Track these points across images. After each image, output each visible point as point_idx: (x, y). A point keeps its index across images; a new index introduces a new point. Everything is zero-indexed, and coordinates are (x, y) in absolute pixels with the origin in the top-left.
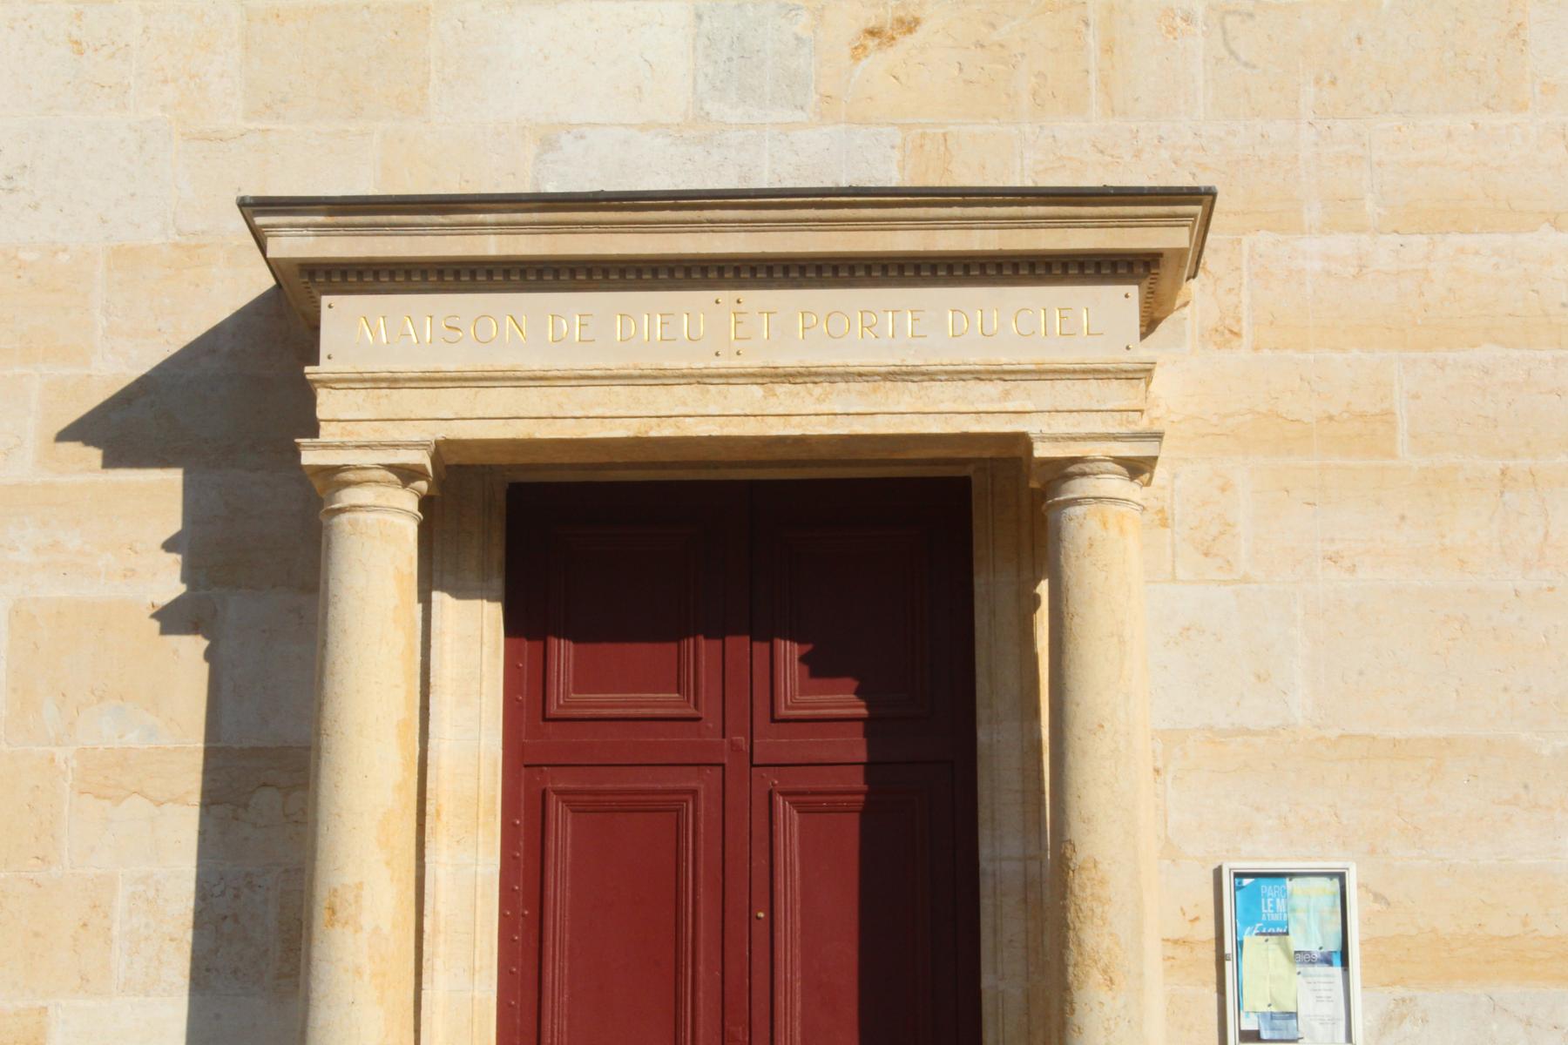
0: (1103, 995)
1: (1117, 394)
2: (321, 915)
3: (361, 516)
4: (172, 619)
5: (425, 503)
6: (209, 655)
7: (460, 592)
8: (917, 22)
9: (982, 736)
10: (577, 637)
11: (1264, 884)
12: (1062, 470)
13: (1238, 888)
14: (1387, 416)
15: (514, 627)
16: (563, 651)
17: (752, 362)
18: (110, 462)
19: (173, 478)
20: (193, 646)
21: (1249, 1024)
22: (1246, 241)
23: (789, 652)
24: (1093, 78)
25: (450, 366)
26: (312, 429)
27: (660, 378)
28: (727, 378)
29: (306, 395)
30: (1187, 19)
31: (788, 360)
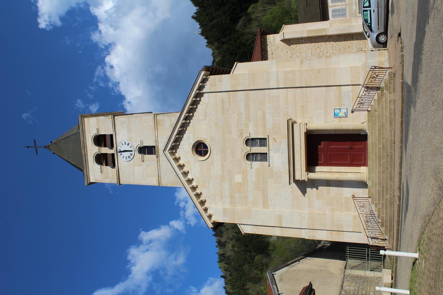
0: (343, 127)
1: (301, 126)
2: (338, 179)
3: (311, 176)
4: (317, 189)
5: (310, 172)
7: (315, 169)
9: (325, 134)
10: (318, 161)
11: (335, 114)
12: (307, 130)
13: (335, 116)
14: (302, 105)
15: (317, 166)
16: (319, 162)
17: (300, 151)
18: (306, 193)
19: (307, 189)
20: (319, 187)
21: (345, 115)
22: (289, 115)
23: (319, 147)
25: (300, 171)
26: (305, 180)
27: (301, 157)
28: (301, 152)
29: (302, 180)
30: (273, 119)
31: (300, 148)
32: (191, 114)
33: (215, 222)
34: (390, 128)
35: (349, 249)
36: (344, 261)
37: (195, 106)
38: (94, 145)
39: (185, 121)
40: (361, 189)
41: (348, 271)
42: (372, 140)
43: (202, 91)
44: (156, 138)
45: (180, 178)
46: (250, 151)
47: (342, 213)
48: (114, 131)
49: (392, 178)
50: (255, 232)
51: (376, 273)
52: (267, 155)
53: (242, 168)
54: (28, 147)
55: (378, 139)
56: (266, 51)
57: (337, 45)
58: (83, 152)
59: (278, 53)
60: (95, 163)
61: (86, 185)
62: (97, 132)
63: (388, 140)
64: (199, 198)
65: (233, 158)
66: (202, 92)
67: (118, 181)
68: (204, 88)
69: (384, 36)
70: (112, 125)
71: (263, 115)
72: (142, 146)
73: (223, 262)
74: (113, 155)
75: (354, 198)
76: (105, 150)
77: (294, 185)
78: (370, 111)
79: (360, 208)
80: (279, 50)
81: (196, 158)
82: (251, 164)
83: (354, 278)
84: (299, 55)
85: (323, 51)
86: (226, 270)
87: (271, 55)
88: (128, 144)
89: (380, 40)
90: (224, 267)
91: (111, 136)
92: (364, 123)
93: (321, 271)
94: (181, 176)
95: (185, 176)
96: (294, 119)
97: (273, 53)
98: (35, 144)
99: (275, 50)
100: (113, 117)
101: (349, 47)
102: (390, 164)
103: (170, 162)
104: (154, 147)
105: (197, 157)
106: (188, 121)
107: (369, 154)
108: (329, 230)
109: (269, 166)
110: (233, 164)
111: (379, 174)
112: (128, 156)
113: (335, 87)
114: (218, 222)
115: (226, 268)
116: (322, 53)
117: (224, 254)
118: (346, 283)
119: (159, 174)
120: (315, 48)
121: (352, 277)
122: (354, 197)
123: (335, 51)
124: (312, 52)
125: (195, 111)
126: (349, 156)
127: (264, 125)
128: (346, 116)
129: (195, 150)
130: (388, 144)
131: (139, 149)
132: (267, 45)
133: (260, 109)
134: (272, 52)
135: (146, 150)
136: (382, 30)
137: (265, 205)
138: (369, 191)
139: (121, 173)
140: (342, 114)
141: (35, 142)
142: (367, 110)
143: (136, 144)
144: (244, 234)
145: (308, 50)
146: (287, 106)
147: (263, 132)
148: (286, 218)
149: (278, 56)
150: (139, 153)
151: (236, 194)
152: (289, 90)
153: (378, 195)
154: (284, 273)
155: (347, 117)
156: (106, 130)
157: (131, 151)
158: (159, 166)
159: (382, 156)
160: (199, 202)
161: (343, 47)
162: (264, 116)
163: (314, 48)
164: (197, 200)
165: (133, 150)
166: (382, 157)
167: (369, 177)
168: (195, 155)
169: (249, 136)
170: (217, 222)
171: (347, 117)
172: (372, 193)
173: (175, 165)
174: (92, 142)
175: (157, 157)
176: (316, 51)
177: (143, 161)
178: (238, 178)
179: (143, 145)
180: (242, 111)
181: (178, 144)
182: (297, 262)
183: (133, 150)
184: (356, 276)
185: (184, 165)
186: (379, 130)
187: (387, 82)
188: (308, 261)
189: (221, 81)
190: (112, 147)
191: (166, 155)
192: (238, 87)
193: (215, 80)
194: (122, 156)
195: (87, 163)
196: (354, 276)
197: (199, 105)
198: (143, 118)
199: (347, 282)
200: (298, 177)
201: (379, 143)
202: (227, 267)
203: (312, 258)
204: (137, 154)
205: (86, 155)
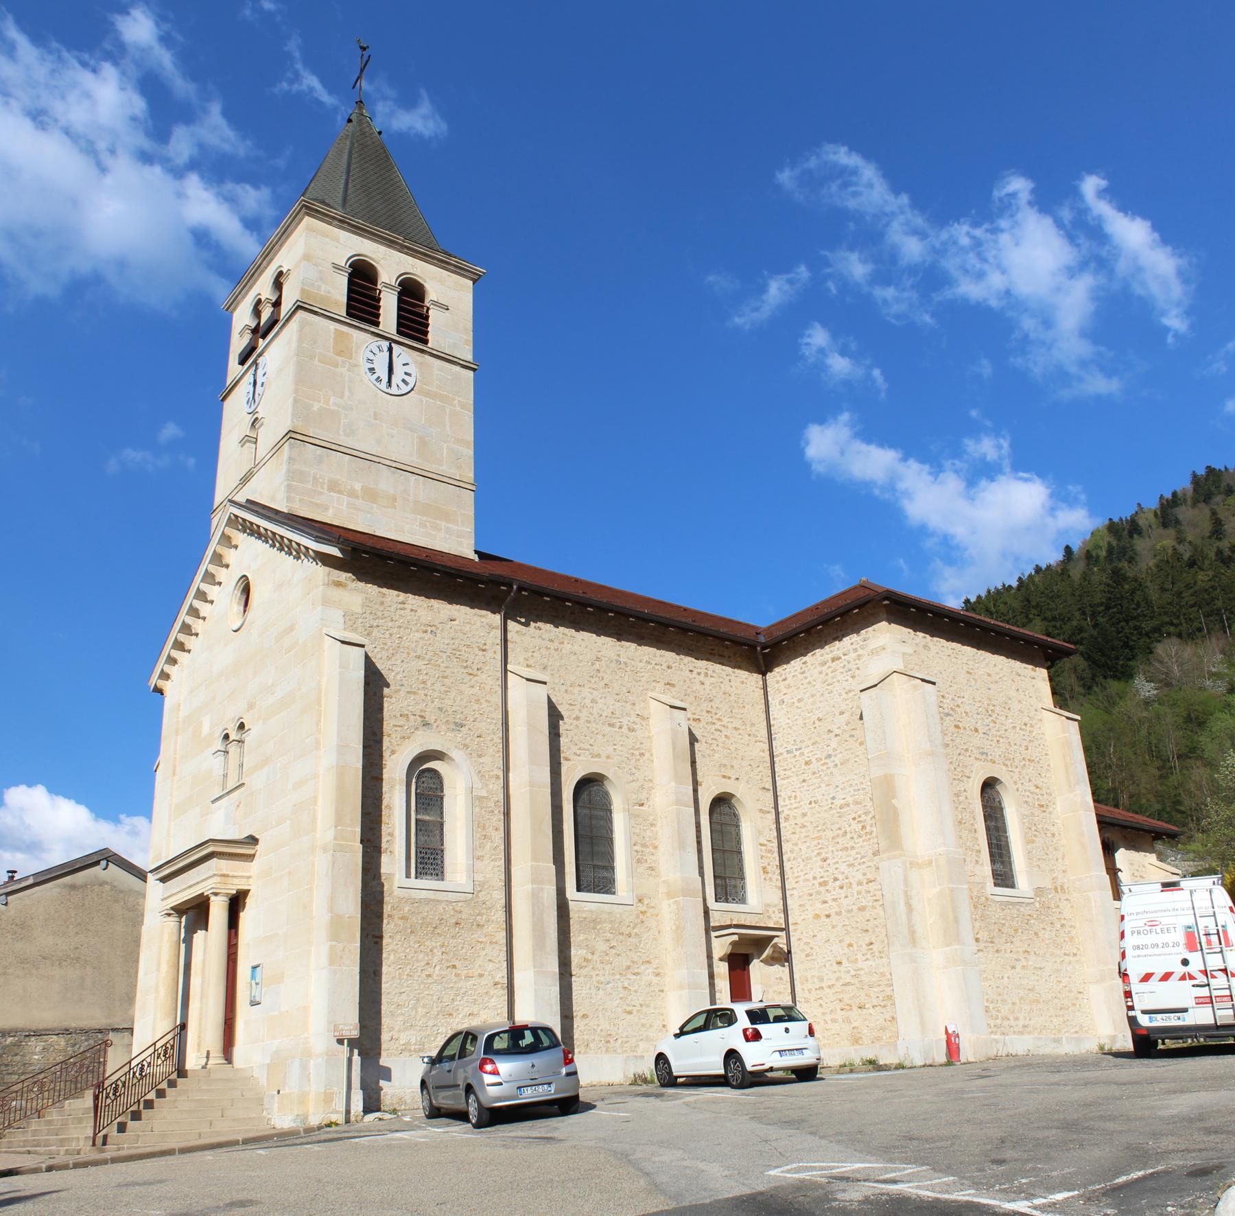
56: (842, 633)
57: (875, 898)
59: (838, 681)
73: (1110, 539)
80: (847, 680)
84: (837, 761)
85: (853, 848)
86: (1088, 556)
87: (831, 656)
90: (1098, 547)
97: (838, 662)
99: (845, 665)
101: (871, 944)
115: (1094, 554)
116: (848, 846)
117: (1140, 533)
120: (860, 816)
123: (855, 894)
124: (848, 805)
132: (858, 632)
134: (839, 658)
145: (854, 790)
149: (830, 681)
161: (868, 921)
163: (859, 813)
176: (851, 821)
202: (1098, 557)
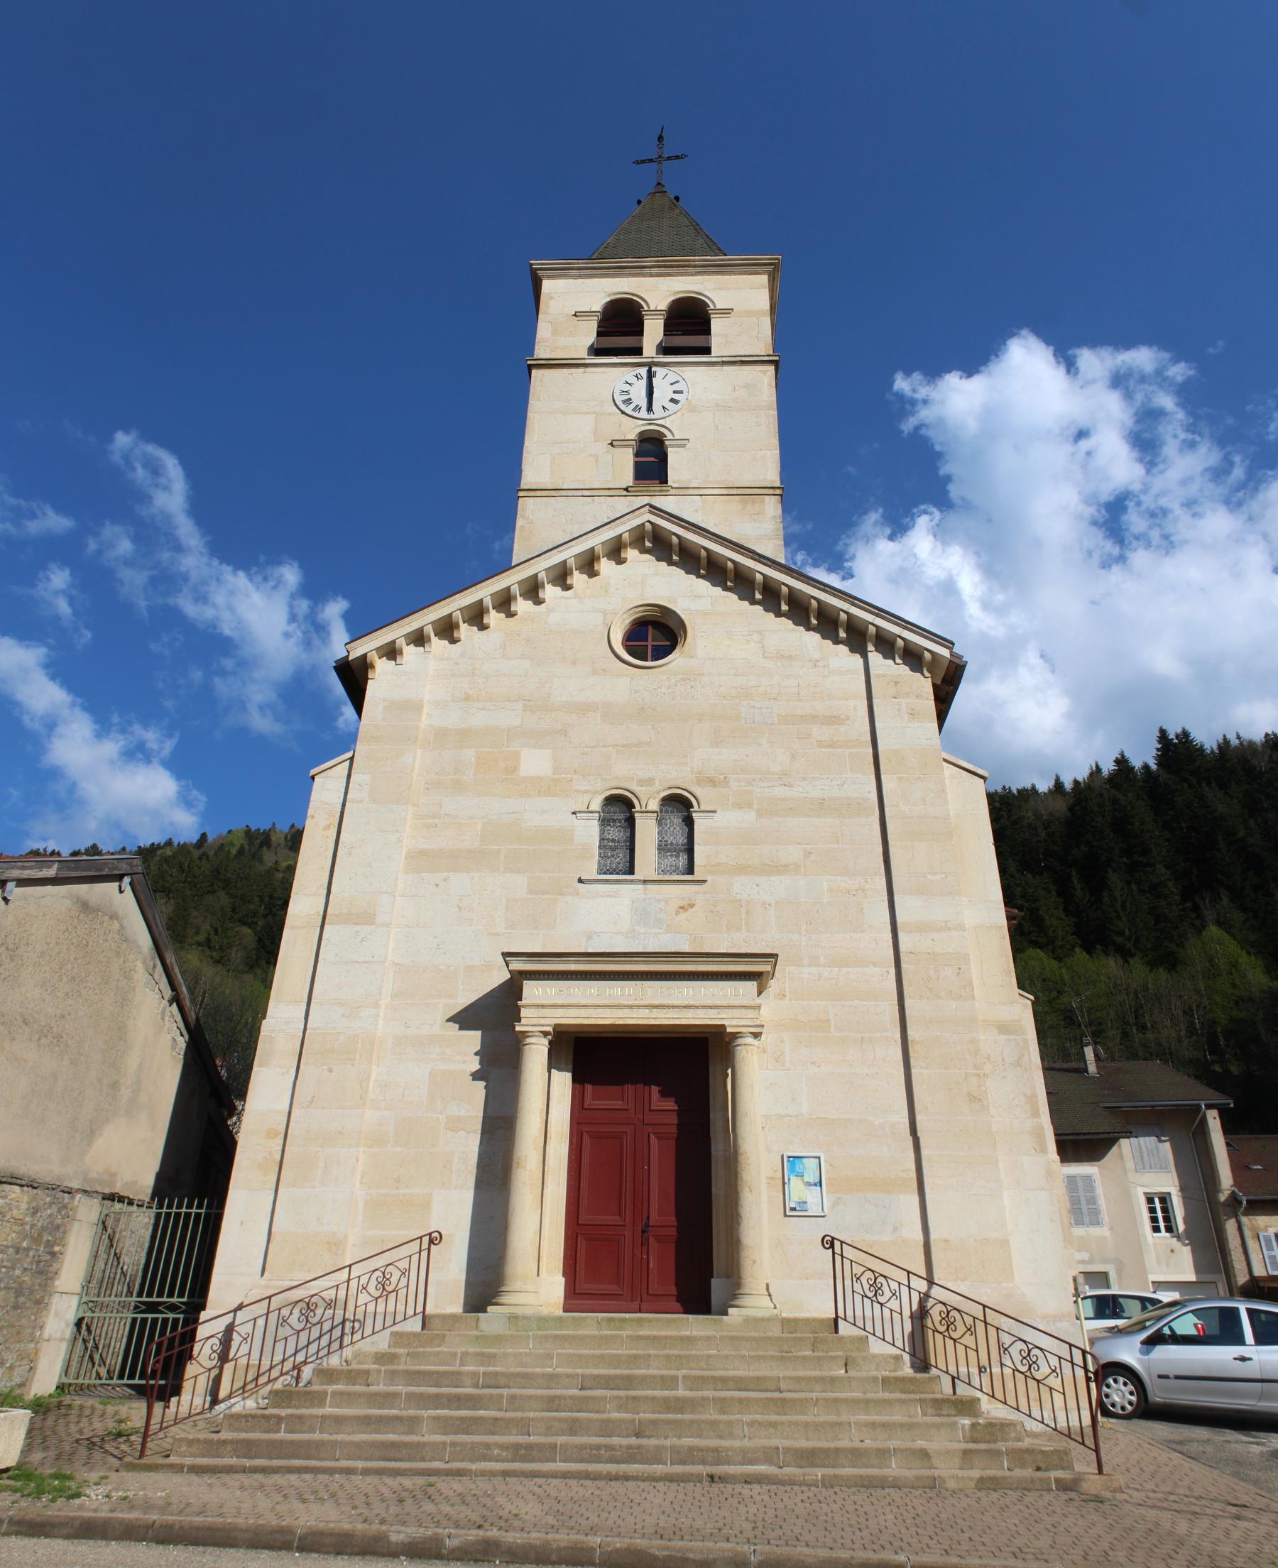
1: (750, 1013)
2: (515, 1165)
3: (535, 1046)
4: (476, 1076)
5: (550, 1043)
6: (486, 1087)
7: (559, 1069)
8: (694, 905)
10: (593, 1083)
12: (735, 1036)
13: (789, 1161)
14: (828, 1021)
15: (574, 1081)
16: (589, 1088)
17: (645, 1003)
18: (460, 1029)
19: (479, 1033)
20: (482, 1084)
21: (793, 1205)
22: (787, 969)
23: (655, 1089)
24: (743, 922)
25: (560, 1002)
26: (519, 1020)
28: (639, 1007)
29: (517, 1010)
31: (656, 1002)
32: (784, 607)
33: (370, 670)
34: (787, 1450)
35: (196, 1213)
36: (150, 1191)
37: (814, 622)
38: (673, 298)
39: (759, 584)
40: (463, 1277)
41: (88, 1212)
42: (701, 1338)
43: (873, 649)
44: (697, 491)
45: (548, 554)
46: (644, 809)
47: (361, 1183)
48: (724, 359)
49: (524, 1459)
50: (313, 817)
51: (64, 1347)
52: (625, 873)
53: (575, 777)
54: (660, 138)
55: (714, 1378)
58: (651, 262)
60: (609, 296)
61: (534, 264)
62: (718, 307)
63: (721, 1437)
64: (466, 618)
65: (617, 746)
66: (870, 647)
67: (542, 362)
68: (885, 657)
69: (1130, 1403)
70: (743, 354)
71: (786, 865)
72: (667, 442)
74: (638, 351)
75: (426, 1240)
76: (653, 331)
77: (500, 976)
78: (836, 1331)
79: (378, 1273)
81: (618, 616)
82: (591, 812)
83: (46, 1237)
88: (673, 401)
89: (1111, 1381)
91: (706, 350)
92: (770, 1295)
93: (115, 1086)
94: (556, 558)
95: (552, 576)
96: (773, 986)
98: (669, 158)
100: (771, 358)
102: (598, 1447)
103: (609, 526)
104: (663, 480)
105: (624, 620)
106: (758, 596)
107: (632, 1320)
108: (292, 1124)
109: (580, 881)
110: (593, 747)
111: (544, 1375)
112: (630, 399)
113: (913, 1166)
114: (369, 681)
118: (26, 1199)
119: (564, 493)
121: (58, 1227)
122: (431, 1242)
125: (796, 624)
126: (613, 1219)
127: (743, 869)
128: (793, 1209)
129: (654, 619)
130: (700, 1436)
131: (656, 436)
133: (808, 854)
135: (652, 459)
136: (1158, 1395)
137: (421, 860)
138: (453, 1318)
139: (571, 374)
140: (797, 1189)
141: (677, 157)
142: (841, 1313)
143: (674, 425)
144: (311, 774)
146: (822, 959)
147: (718, 864)
148: (362, 940)
150: (641, 433)
151: (473, 750)
152: (888, 972)
153: (437, 1373)
154: (122, 927)
155: (786, 1215)
156: (722, 335)
157: (650, 409)
158: (592, 492)
159: (635, 1398)
160: (451, 613)
162: (782, 869)
164: (460, 609)
165: (652, 416)
166: (627, 1398)
167: (524, 1318)
168: (631, 615)
169: (703, 808)
170: (370, 676)
171: (788, 1214)
172: (444, 1336)
173: (596, 541)
174: (682, 292)
175: (626, 489)
177: (611, 444)
178: (535, 762)
179: (672, 446)
180: (798, 786)
181: (675, 558)
182: (168, 993)
183: (652, 416)
184: (56, 1249)
185: (596, 576)
186: (758, 1383)
187: (1013, 1435)
188: (169, 1037)
189: (912, 714)
190: (665, 350)
191: (637, 512)
192: (894, 776)
193: (918, 697)
194: (633, 380)
195: (611, 271)
196: (62, 1241)
197: (818, 636)
198: (769, 453)
199: (28, 1203)
200: (533, 991)
201: (697, 1382)
203: (182, 1057)
204: (641, 427)
205: (639, 271)
